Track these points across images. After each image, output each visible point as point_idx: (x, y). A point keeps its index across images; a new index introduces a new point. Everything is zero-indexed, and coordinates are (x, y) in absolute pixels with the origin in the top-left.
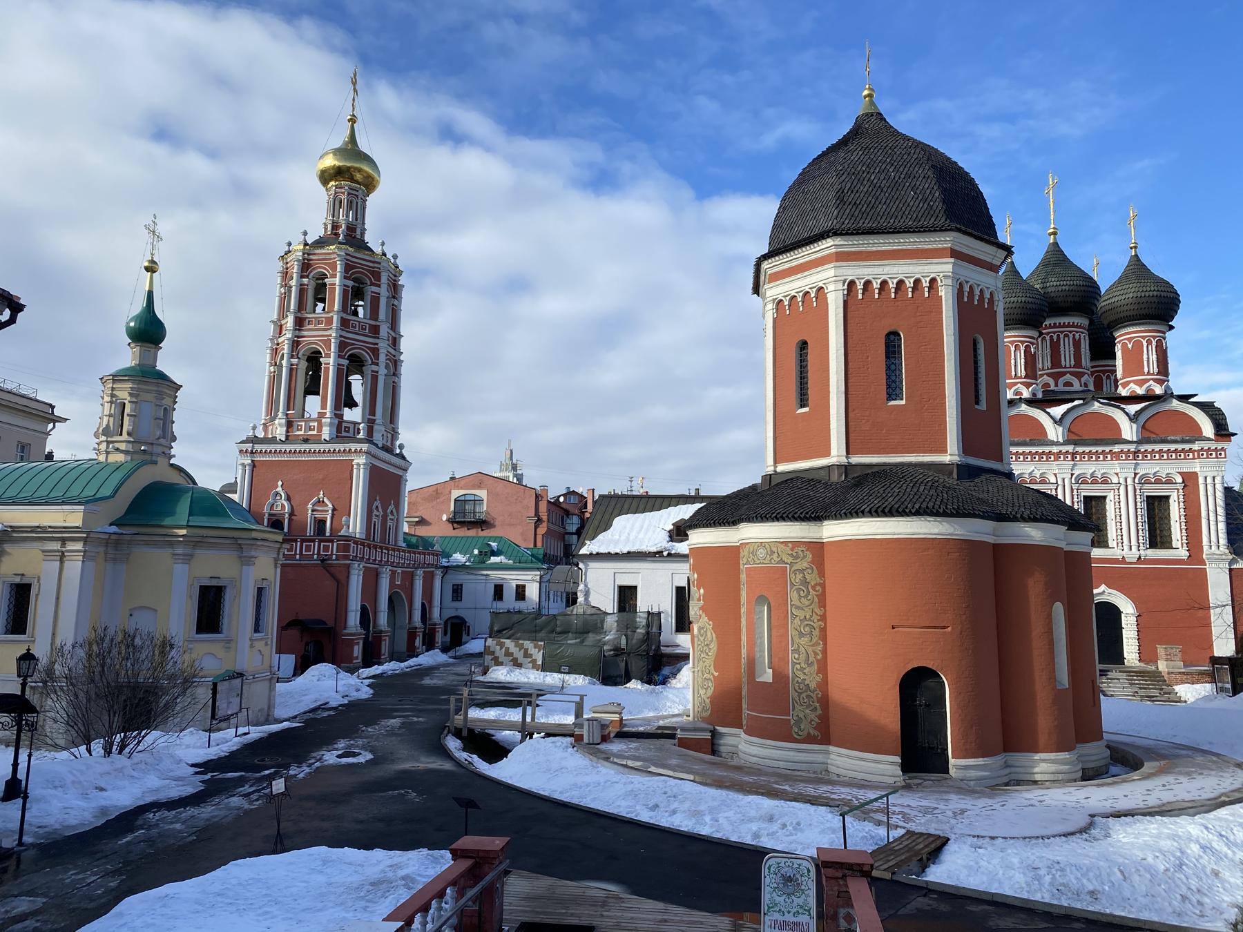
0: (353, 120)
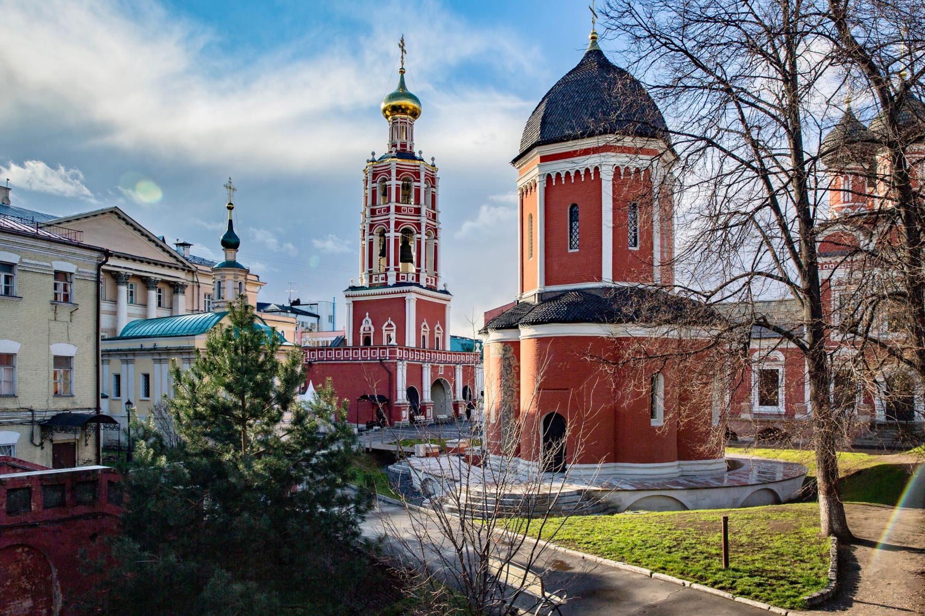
0: (402, 72)
